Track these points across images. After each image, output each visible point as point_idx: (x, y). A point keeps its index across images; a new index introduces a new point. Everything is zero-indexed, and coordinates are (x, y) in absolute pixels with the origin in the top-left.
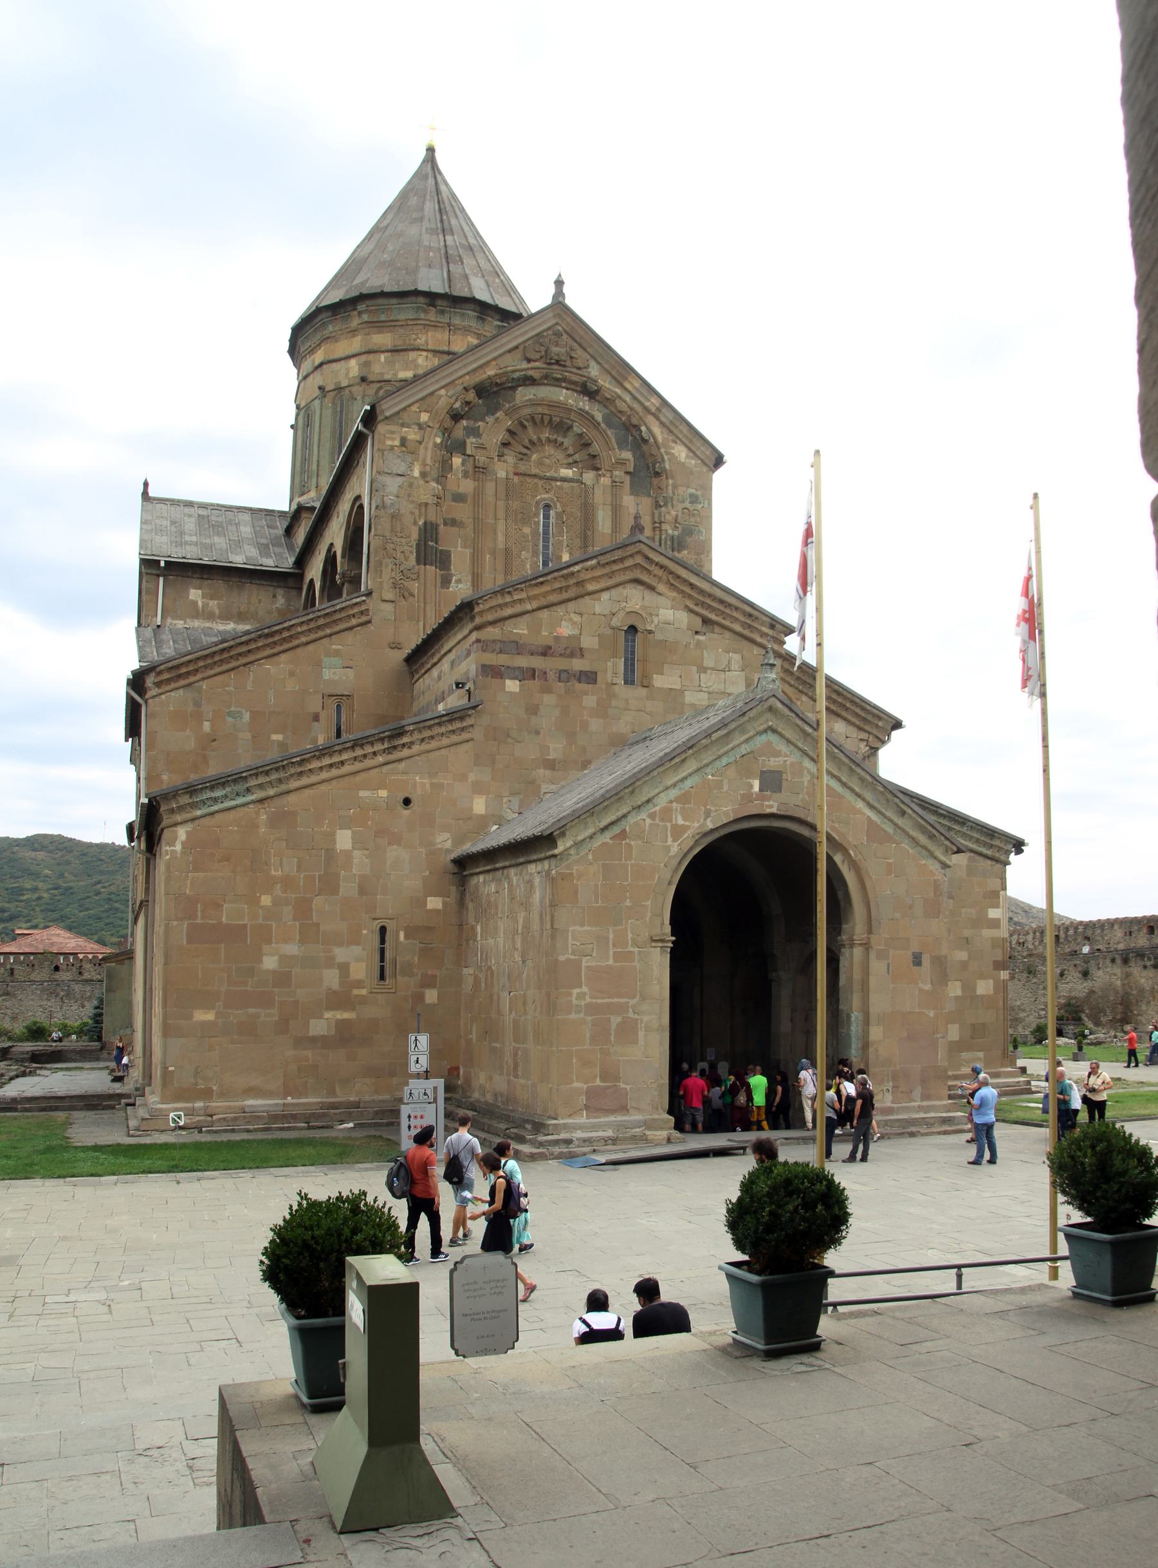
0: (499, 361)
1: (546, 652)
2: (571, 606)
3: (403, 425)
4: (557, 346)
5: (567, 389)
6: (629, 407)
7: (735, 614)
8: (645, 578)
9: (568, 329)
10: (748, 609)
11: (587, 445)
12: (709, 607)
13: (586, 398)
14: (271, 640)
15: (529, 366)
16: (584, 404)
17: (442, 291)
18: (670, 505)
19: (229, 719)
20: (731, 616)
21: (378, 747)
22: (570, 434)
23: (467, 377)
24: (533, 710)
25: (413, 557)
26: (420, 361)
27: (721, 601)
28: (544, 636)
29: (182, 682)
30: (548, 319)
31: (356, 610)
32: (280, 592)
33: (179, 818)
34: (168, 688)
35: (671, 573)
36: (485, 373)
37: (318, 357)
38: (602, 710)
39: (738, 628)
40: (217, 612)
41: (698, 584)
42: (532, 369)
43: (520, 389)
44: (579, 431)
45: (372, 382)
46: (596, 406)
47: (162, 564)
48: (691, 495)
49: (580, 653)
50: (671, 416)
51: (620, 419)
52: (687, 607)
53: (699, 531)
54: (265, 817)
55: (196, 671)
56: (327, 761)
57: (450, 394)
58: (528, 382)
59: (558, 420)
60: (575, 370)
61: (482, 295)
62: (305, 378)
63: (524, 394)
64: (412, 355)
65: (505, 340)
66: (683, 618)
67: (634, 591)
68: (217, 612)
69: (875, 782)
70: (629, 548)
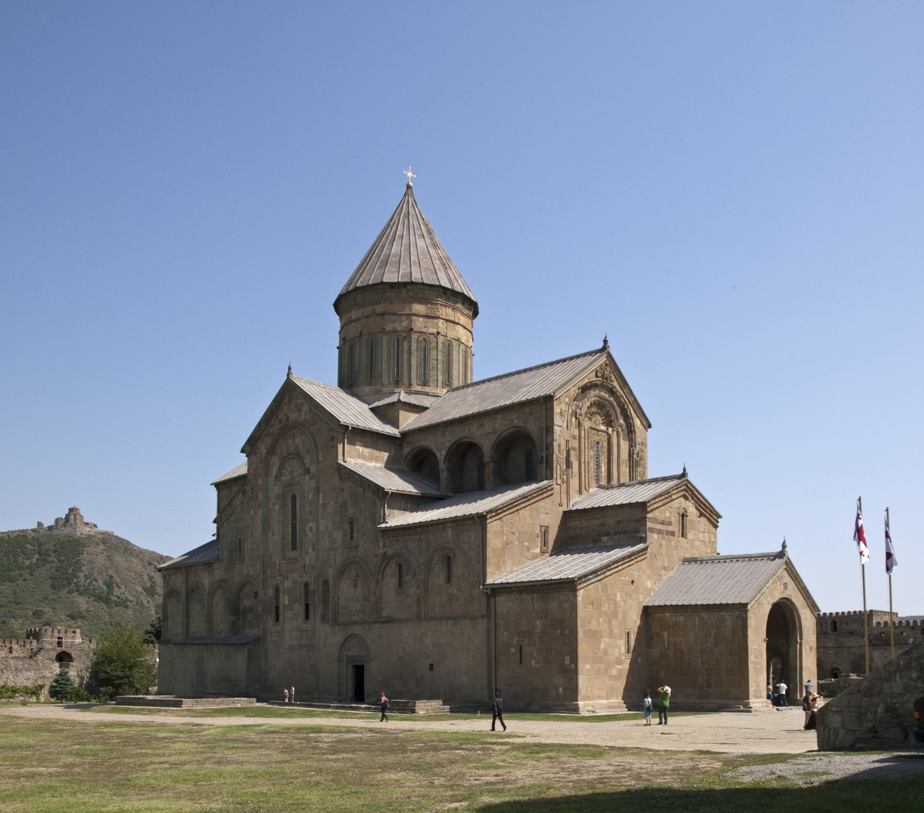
1: (663, 523)
2: (669, 504)
11: (610, 416)
14: (525, 500)
17: (451, 288)
19: (512, 535)
21: (628, 560)
24: (660, 546)
25: (564, 464)
26: (440, 324)
28: (661, 518)
29: (498, 517)
31: (550, 488)
32: (392, 447)
33: (581, 586)
34: (494, 519)
37: (379, 309)
38: (676, 548)
40: (367, 455)
45: (416, 332)
47: (350, 428)
49: (670, 524)
54: (600, 586)
55: (501, 513)
56: (616, 565)
61: (466, 293)
62: (367, 317)
64: (436, 321)
66: (695, 509)
68: (367, 455)
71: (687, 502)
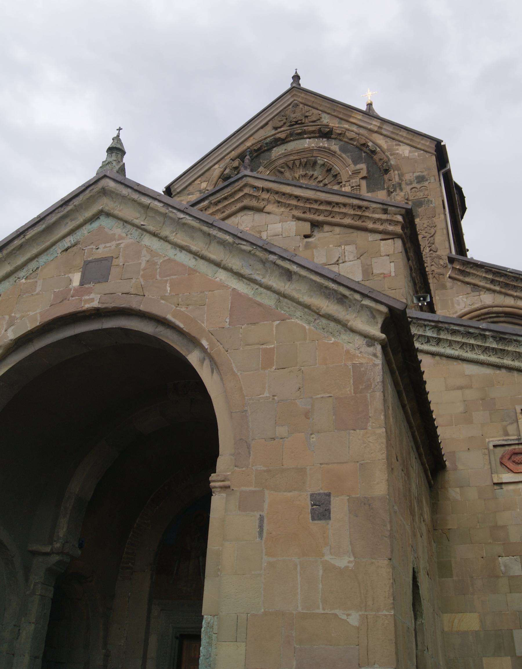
0: (255, 136)
3: (189, 195)
4: (294, 113)
5: (310, 138)
6: (356, 133)
7: (344, 210)
8: (254, 203)
9: (303, 101)
10: (356, 202)
11: (329, 170)
12: (317, 211)
13: (325, 140)
15: (277, 131)
16: (324, 143)
18: (398, 189)
20: (340, 213)
22: (317, 167)
23: (233, 152)
27: (329, 203)
30: (288, 100)
35: (277, 193)
36: (245, 145)
39: (347, 221)
41: (302, 194)
42: (278, 133)
43: (274, 149)
44: (322, 162)
46: (333, 142)
48: (417, 177)
50: (390, 128)
51: (353, 145)
52: (294, 217)
53: (428, 201)
57: (221, 166)
58: (279, 143)
59: (305, 160)
60: (311, 124)
63: (277, 152)
65: (257, 122)
66: (292, 226)
67: (245, 217)
69: (238, 241)
70: (237, 184)
71: (258, 217)
